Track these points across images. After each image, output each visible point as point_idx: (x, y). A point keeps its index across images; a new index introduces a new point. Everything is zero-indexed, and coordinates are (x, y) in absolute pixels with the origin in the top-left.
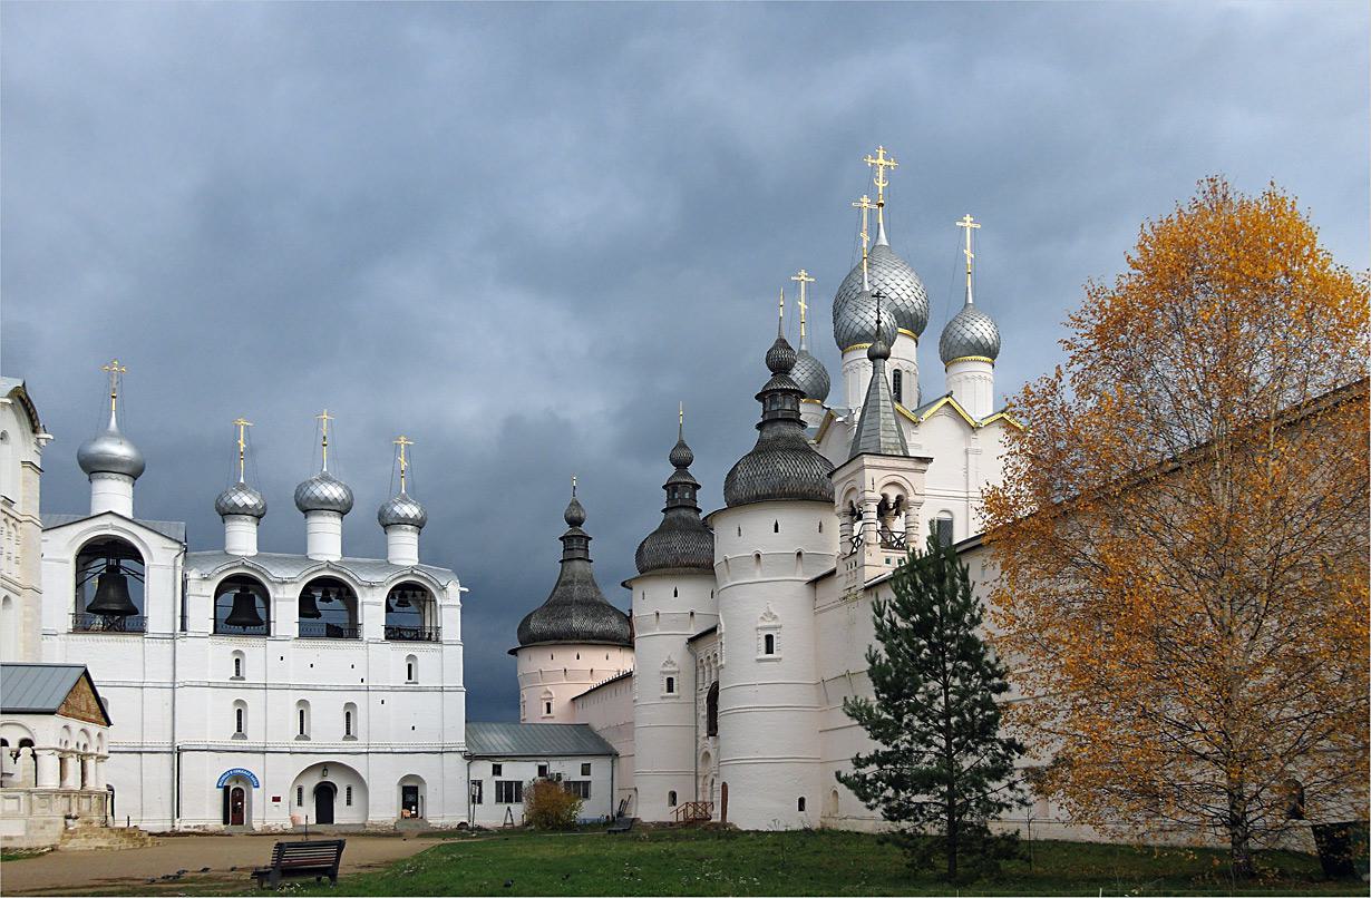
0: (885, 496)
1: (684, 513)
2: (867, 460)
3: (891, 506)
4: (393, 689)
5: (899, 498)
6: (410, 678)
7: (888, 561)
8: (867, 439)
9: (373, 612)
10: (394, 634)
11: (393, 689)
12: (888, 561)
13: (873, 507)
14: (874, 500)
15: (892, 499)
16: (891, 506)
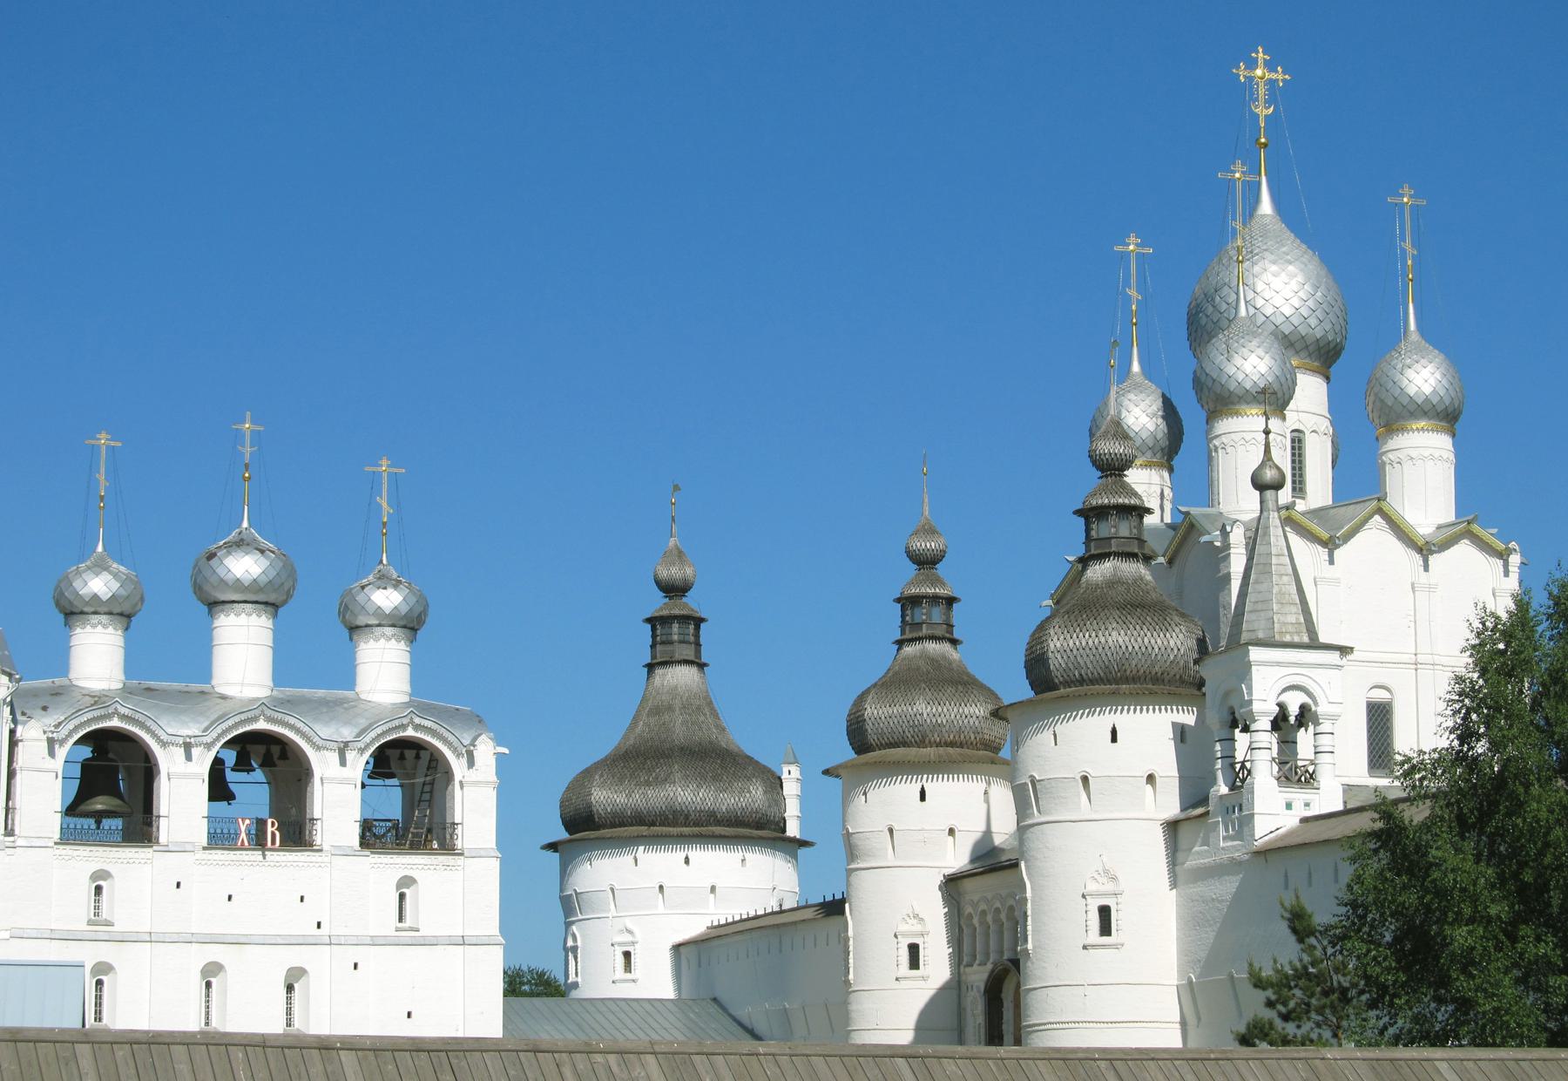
0: (1282, 706)
1: (946, 647)
2: (1255, 654)
3: (1292, 720)
4: (375, 942)
5: (1304, 709)
6: (401, 920)
7: (1289, 806)
8: (1253, 617)
9: (339, 793)
10: (373, 836)
11: (375, 942)
12: (1289, 806)
13: (1264, 723)
14: (1264, 714)
15: (1293, 711)
16: (1292, 720)
